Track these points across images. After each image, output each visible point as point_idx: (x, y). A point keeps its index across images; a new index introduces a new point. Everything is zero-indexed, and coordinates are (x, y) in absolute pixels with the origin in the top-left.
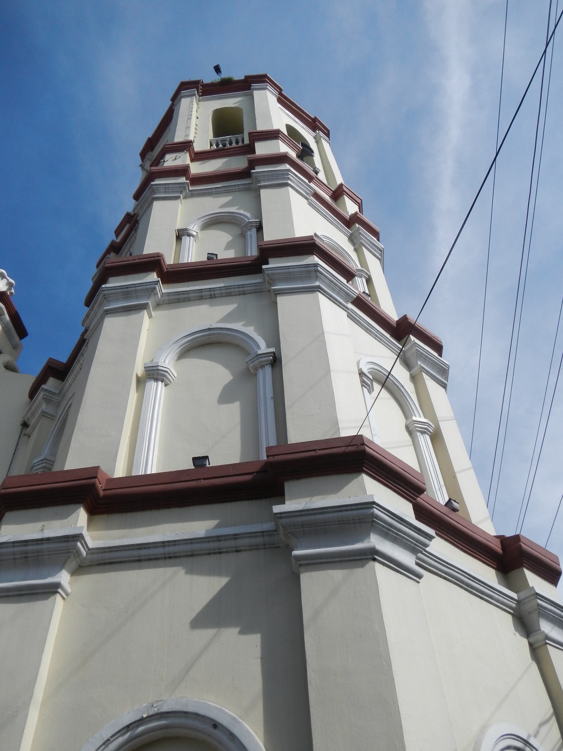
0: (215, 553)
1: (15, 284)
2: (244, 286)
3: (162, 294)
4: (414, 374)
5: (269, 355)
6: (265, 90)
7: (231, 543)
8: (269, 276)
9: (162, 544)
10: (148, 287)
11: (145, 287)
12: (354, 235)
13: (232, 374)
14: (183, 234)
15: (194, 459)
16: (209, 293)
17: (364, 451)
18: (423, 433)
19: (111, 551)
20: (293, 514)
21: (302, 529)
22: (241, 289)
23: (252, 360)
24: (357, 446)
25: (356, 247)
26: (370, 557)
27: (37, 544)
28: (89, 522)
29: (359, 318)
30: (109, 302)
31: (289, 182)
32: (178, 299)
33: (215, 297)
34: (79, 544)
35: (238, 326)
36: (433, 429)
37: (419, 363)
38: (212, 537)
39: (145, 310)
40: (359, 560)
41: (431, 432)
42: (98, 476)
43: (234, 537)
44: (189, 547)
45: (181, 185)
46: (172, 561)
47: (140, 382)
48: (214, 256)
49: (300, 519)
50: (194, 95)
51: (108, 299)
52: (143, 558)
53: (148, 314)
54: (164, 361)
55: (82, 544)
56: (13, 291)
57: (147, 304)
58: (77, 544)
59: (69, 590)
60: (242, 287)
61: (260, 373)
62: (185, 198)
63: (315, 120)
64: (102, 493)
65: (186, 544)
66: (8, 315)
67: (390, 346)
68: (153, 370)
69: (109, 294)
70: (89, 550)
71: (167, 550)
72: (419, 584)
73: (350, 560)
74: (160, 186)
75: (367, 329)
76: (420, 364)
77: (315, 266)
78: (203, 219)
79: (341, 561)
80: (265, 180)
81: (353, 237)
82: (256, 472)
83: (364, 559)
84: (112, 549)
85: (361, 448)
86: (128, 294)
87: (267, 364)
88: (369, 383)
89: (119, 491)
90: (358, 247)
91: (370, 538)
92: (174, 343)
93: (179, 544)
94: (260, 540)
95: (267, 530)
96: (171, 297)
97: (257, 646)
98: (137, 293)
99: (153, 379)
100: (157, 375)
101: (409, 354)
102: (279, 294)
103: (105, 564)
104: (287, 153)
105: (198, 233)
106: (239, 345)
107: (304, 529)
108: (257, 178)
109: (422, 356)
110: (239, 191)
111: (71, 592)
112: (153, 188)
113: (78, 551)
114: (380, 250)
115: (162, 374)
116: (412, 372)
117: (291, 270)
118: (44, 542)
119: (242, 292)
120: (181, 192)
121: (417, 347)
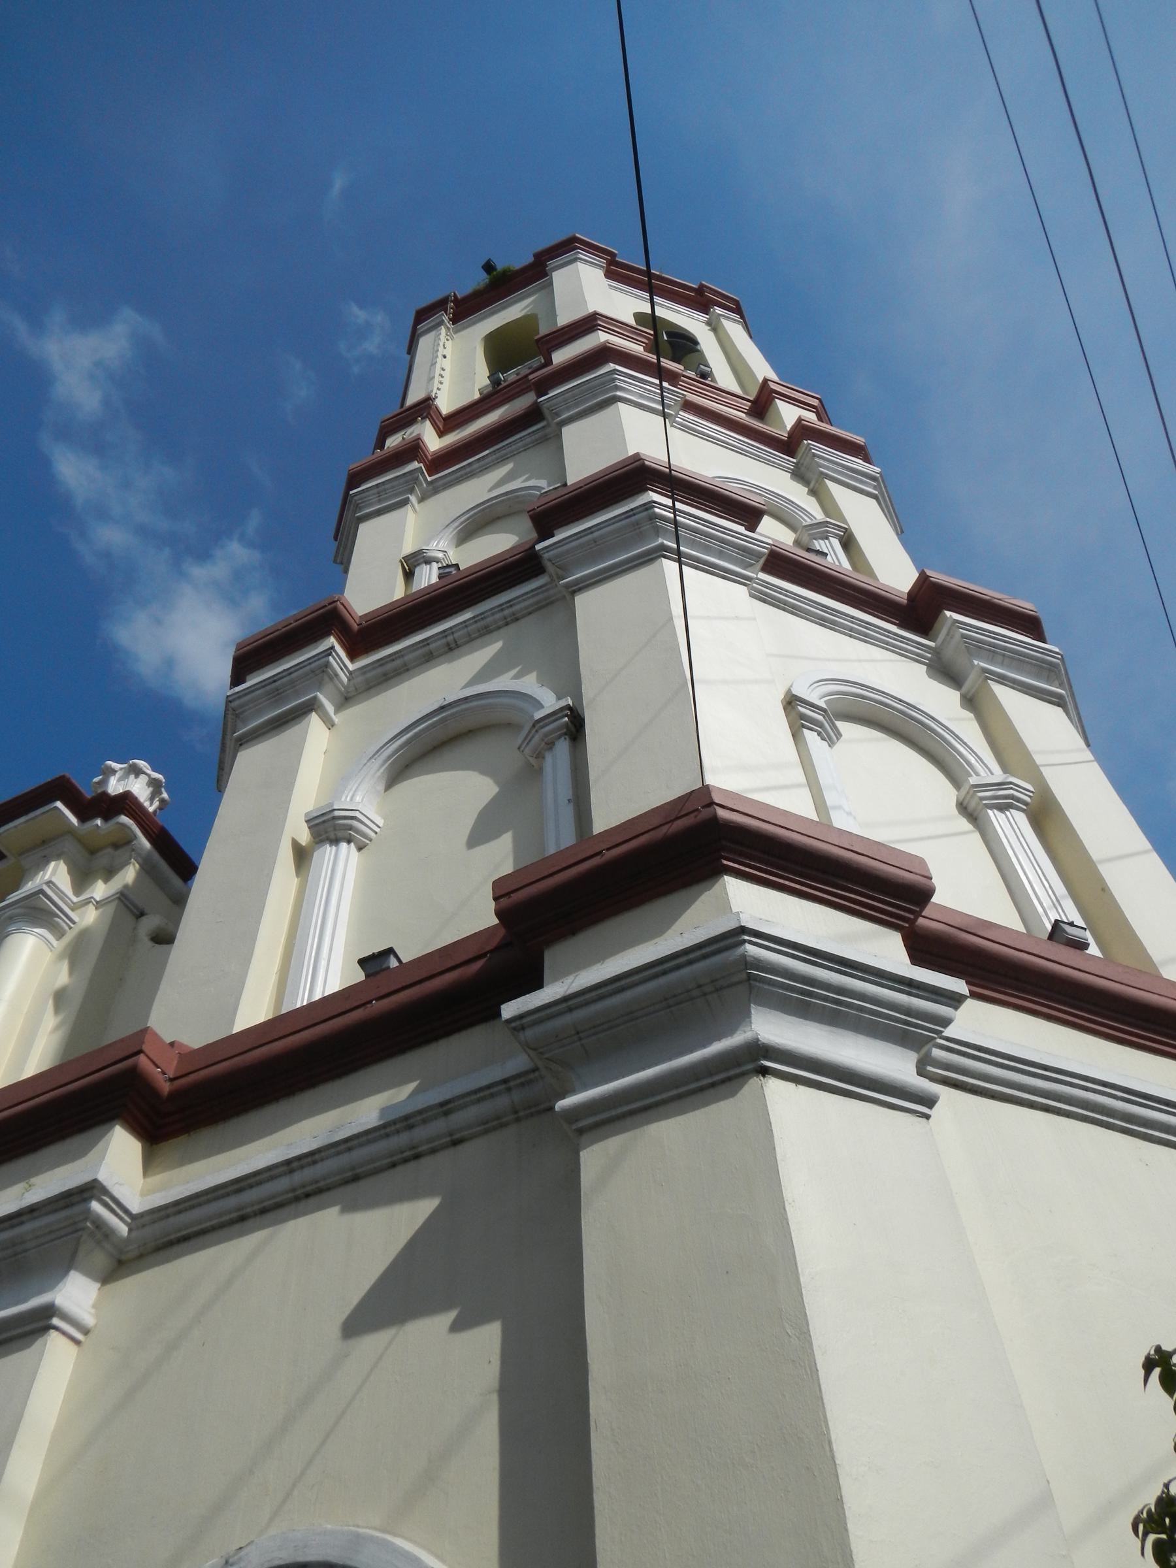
0: (406, 1161)
1: (164, 780)
2: (512, 603)
3: (351, 673)
4: (974, 690)
5: (560, 715)
6: (575, 264)
7: (439, 1126)
8: (553, 562)
9: (285, 1168)
10: (313, 665)
11: (308, 668)
12: (802, 464)
13: (497, 782)
14: (416, 564)
15: (363, 962)
16: (444, 641)
17: (715, 818)
18: (1002, 808)
19: (180, 1212)
20: (549, 1011)
21: (578, 1043)
22: (506, 612)
23: (528, 739)
24: (695, 813)
25: (812, 485)
26: (750, 1066)
27: (12, 1227)
28: (149, 1163)
29: (795, 599)
30: (245, 722)
31: (619, 393)
32: (385, 674)
33: (458, 646)
34: (95, 1206)
35: (504, 682)
36: (1031, 794)
37: (976, 662)
38: (394, 1122)
39: (314, 713)
40: (723, 1081)
41: (1026, 804)
42: (144, 1048)
43: (441, 1110)
44: (344, 1160)
45: (409, 477)
46: (312, 1201)
47: (302, 856)
48: (452, 569)
49: (568, 1019)
50: (441, 323)
51: (241, 716)
52: (249, 1210)
53: (324, 722)
54: (351, 800)
55: (106, 1205)
56: (165, 795)
57: (315, 698)
58: (89, 1209)
59: (89, 1320)
60: (508, 607)
61: (549, 757)
62: (421, 500)
63: (701, 290)
64: (165, 1088)
65: (338, 1153)
66: (144, 835)
67: (894, 646)
68: (324, 822)
69: (241, 706)
70: (137, 1221)
71: (298, 1178)
72: (931, 1120)
73: (701, 1089)
74: (367, 494)
75: (823, 619)
76: (978, 664)
77: (647, 509)
78: (456, 524)
79: (680, 1097)
80: (568, 409)
81: (803, 469)
82: (491, 951)
83: (738, 1076)
84: (182, 1207)
85: (705, 814)
86: (278, 694)
87: (559, 737)
88: (820, 718)
89: (203, 1073)
90: (817, 484)
91: (751, 1023)
92: (371, 758)
93: (322, 1160)
94: (502, 1102)
95: (514, 1072)
96: (369, 675)
97: (490, 1362)
98: (295, 686)
99: (328, 842)
100: (335, 830)
101: (948, 653)
102: (580, 590)
103: (171, 1244)
104: (607, 342)
105: (446, 552)
106: (509, 724)
107: (583, 1042)
108: (553, 410)
109: (980, 648)
110: (525, 450)
111: (96, 1325)
112: (356, 501)
113: (99, 1224)
114: (874, 479)
115: (344, 825)
116: (967, 686)
117: (596, 534)
118: (24, 1218)
119: (511, 616)
120: (412, 491)
121: (961, 630)
